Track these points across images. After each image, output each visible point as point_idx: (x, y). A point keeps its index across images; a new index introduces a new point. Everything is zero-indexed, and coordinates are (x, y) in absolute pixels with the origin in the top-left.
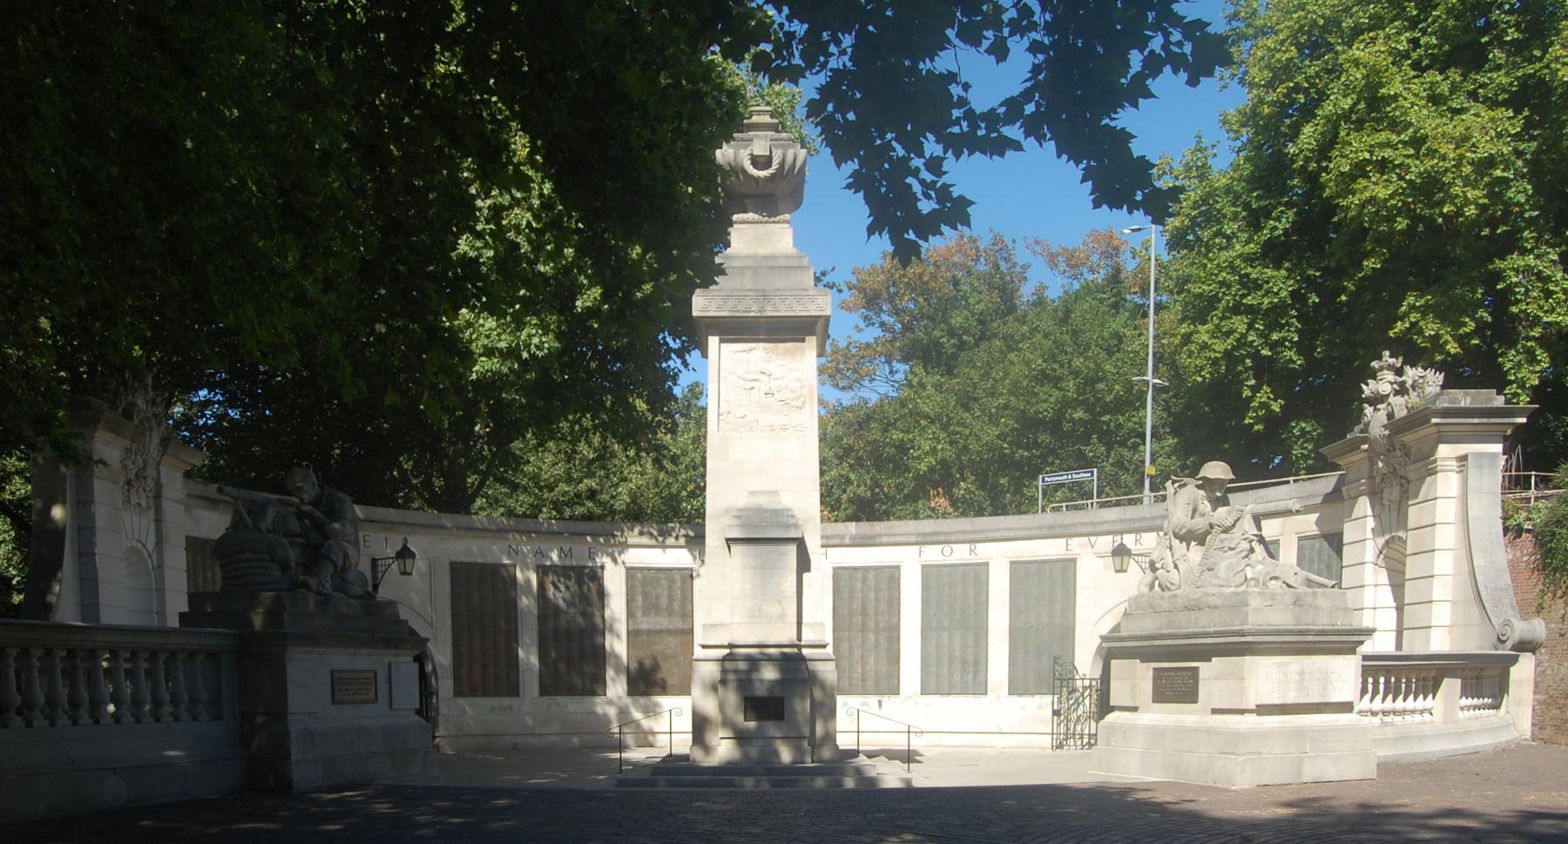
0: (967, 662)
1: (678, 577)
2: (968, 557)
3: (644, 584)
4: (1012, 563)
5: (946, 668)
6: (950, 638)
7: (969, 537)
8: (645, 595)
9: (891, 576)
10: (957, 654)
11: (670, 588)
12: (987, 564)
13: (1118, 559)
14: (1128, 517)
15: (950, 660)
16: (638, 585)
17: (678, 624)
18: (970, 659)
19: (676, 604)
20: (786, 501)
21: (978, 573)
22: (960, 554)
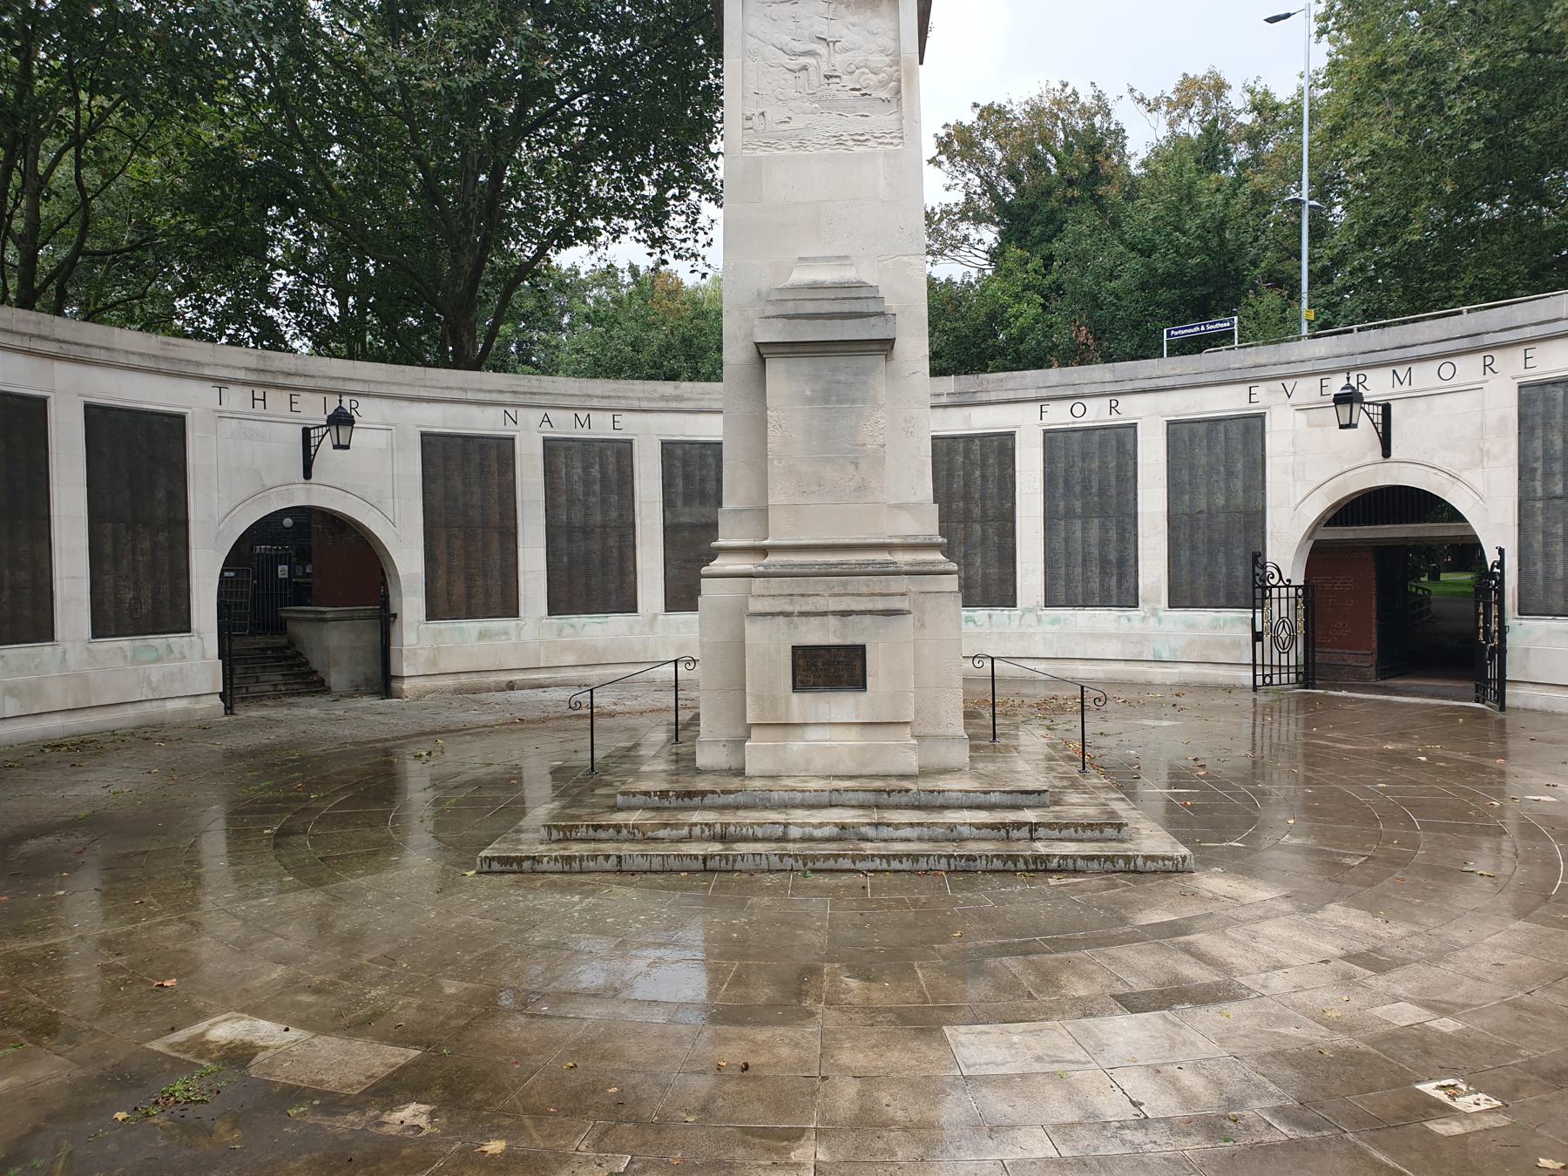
0: (1109, 562)
2: (1108, 417)
3: (685, 463)
4: (1169, 423)
5: (1078, 570)
6: (1084, 529)
7: (1109, 388)
8: (687, 477)
9: (1002, 446)
10: (1095, 551)
12: (1134, 426)
13: (1344, 410)
14: (1344, 350)
15: (1084, 560)
16: (678, 464)
18: (1113, 557)
21: (1122, 439)
22: (1096, 413)
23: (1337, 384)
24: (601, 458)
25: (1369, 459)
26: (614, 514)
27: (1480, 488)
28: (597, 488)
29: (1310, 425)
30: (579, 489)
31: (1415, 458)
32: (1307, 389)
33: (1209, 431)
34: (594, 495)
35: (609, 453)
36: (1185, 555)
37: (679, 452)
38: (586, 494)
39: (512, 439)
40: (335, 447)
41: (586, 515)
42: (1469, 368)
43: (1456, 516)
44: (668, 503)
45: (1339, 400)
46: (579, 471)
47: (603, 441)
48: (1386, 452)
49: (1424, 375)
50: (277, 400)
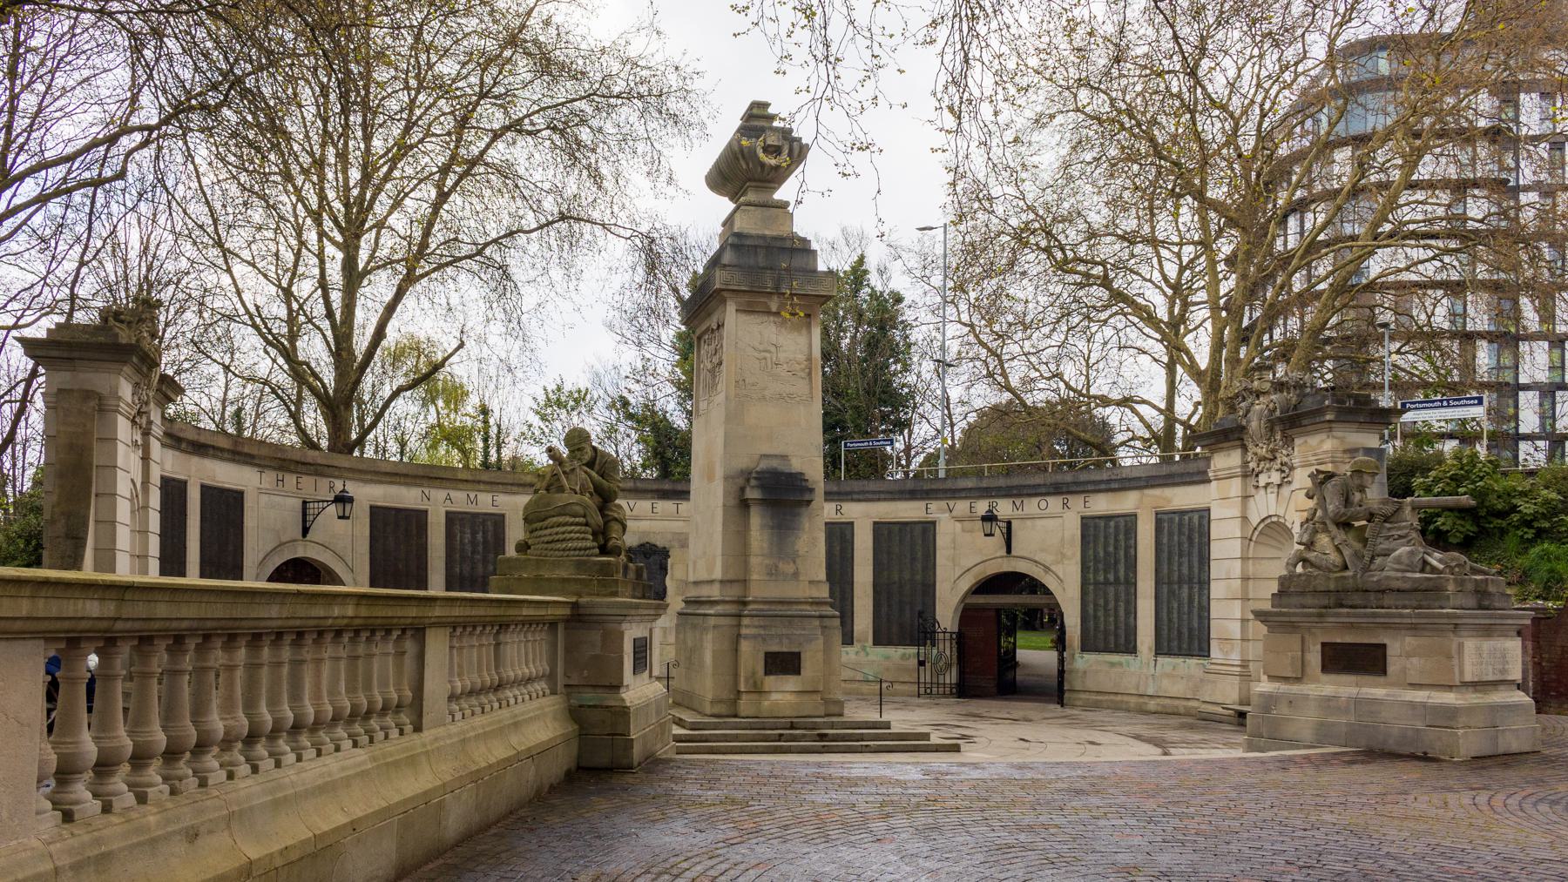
4: (875, 523)
12: (852, 523)
13: (987, 525)
20: (796, 465)
23: (982, 507)
25: (998, 554)
27: (1061, 576)
28: (480, 548)
29: (963, 531)
30: (469, 548)
31: (1025, 555)
32: (961, 506)
33: (900, 530)
36: (884, 610)
38: (473, 552)
39: (426, 511)
40: (339, 518)
42: (1054, 503)
43: (1048, 592)
45: (984, 519)
47: (486, 514)
48: (1009, 550)
49: (1032, 505)
50: (291, 479)
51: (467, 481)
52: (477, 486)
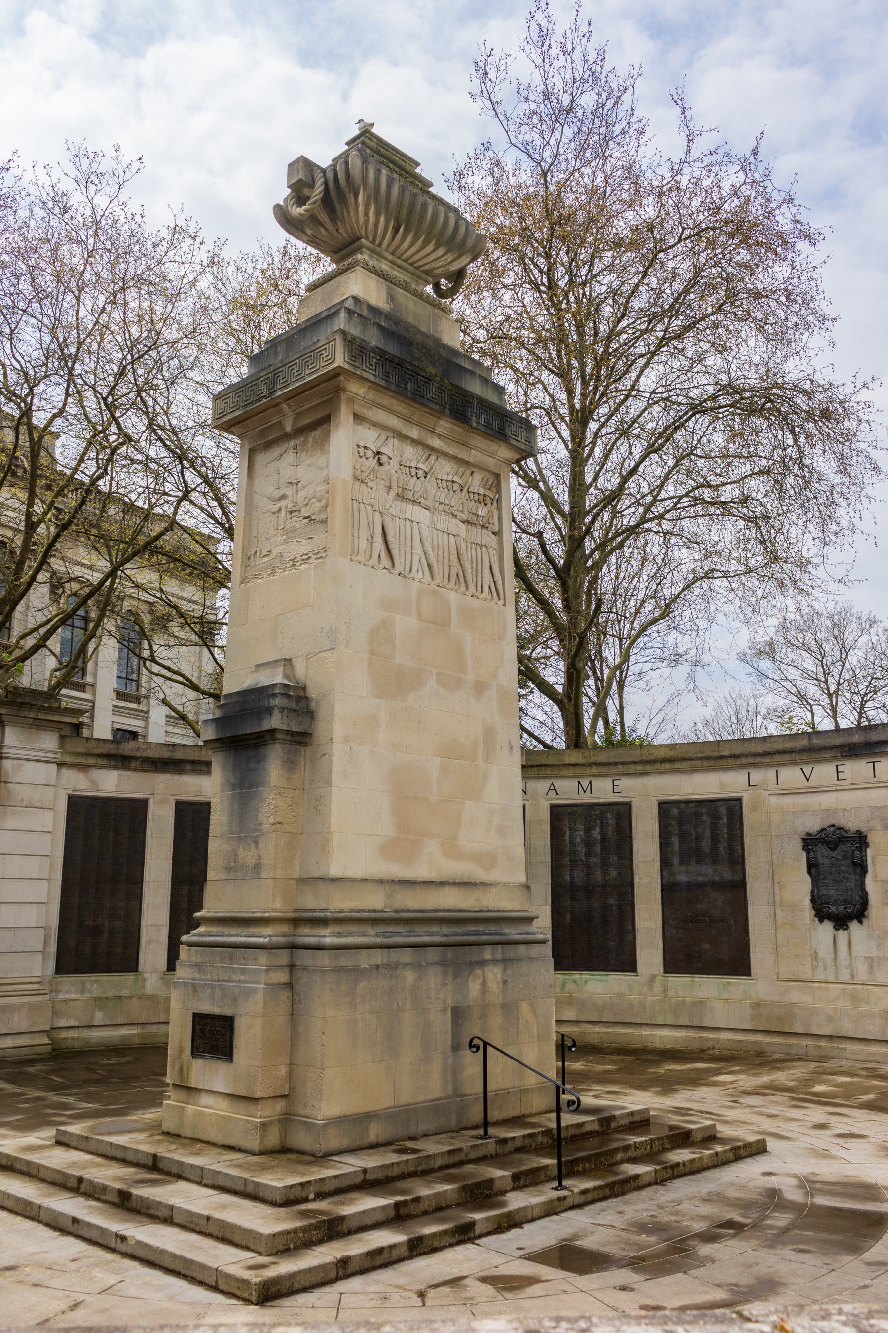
1: (723, 810)
3: (681, 822)
8: (682, 836)
11: (714, 827)
16: (674, 823)
17: (726, 874)
19: (722, 847)
24: (602, 822)
26: (613, 873)
28: (598, 848)
30: (582, 850)
34: (595, 855)
35: (609, 815)
37: (675, 811)
38: (588, 855)
41: (588, 875)
44: (665, 862)
46: (582, 833)
51: (574, 765)
52: (588, 770)
